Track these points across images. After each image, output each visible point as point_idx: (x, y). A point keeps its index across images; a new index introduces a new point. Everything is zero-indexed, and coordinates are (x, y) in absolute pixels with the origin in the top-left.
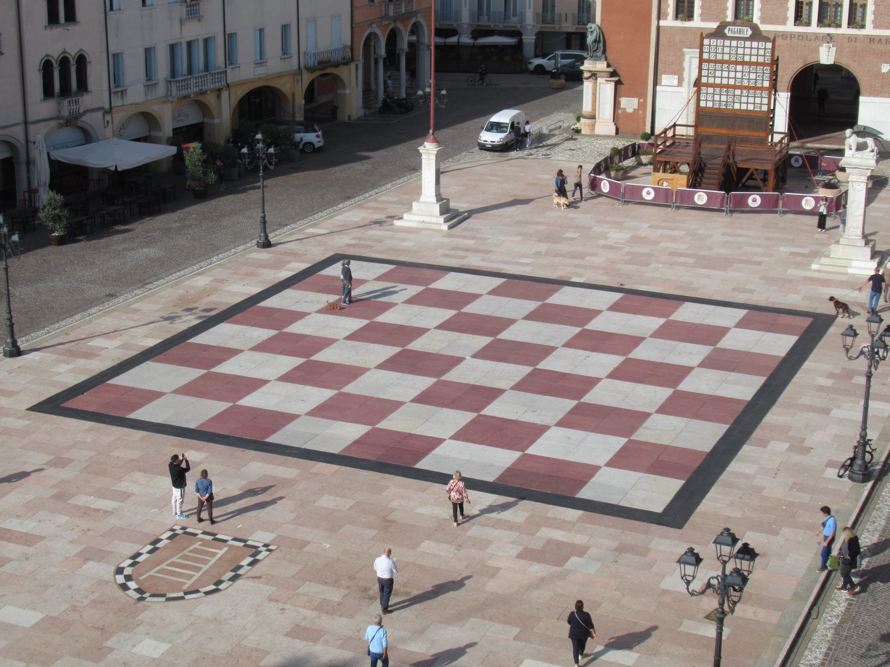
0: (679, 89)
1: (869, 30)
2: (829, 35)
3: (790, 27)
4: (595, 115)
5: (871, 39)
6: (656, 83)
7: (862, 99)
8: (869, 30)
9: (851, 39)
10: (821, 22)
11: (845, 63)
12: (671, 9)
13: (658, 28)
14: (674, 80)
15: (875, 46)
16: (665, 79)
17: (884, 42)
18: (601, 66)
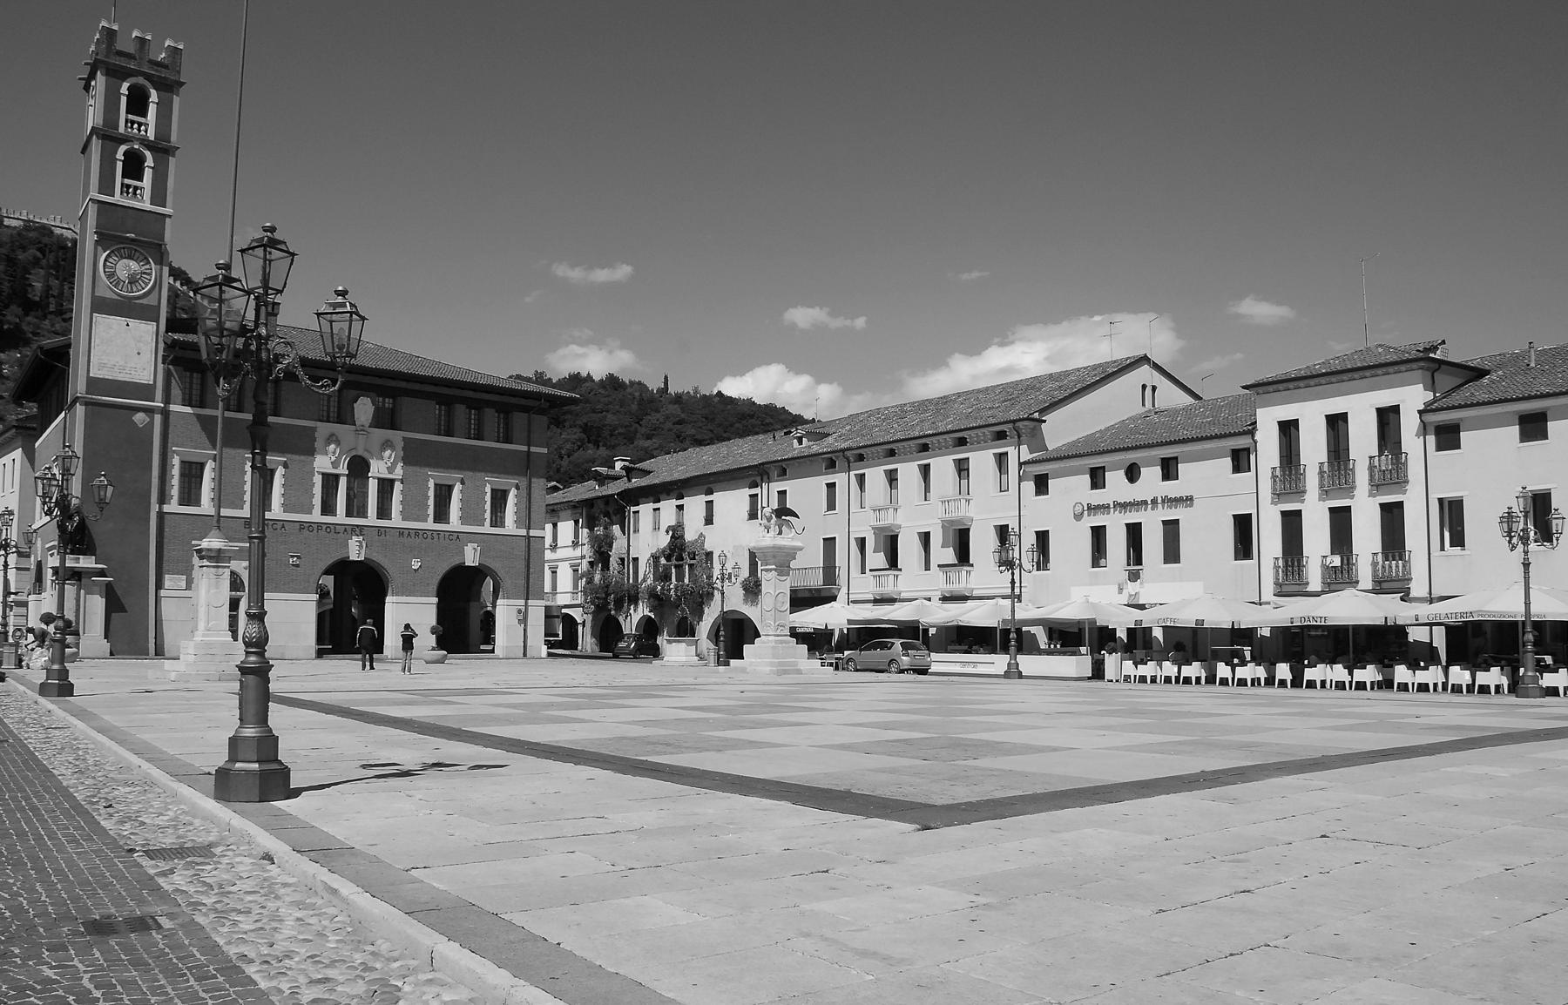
0: (187, 593)
1: (396, 520)
2: (357, 526)
3: (316, 516)
4: (79, 631)
5: (401, 532)
6: (159, 585)
7: (388, 599)
8: (396, 520)
9: (380, 530)
10: (349, 514)
11: (378, 558)
12: (175, 492)
13: (161, 515)
14: (182, 581)
15: (404, 540)
16: (168, 580)
17: (413, 535)
18: (86, 562)
